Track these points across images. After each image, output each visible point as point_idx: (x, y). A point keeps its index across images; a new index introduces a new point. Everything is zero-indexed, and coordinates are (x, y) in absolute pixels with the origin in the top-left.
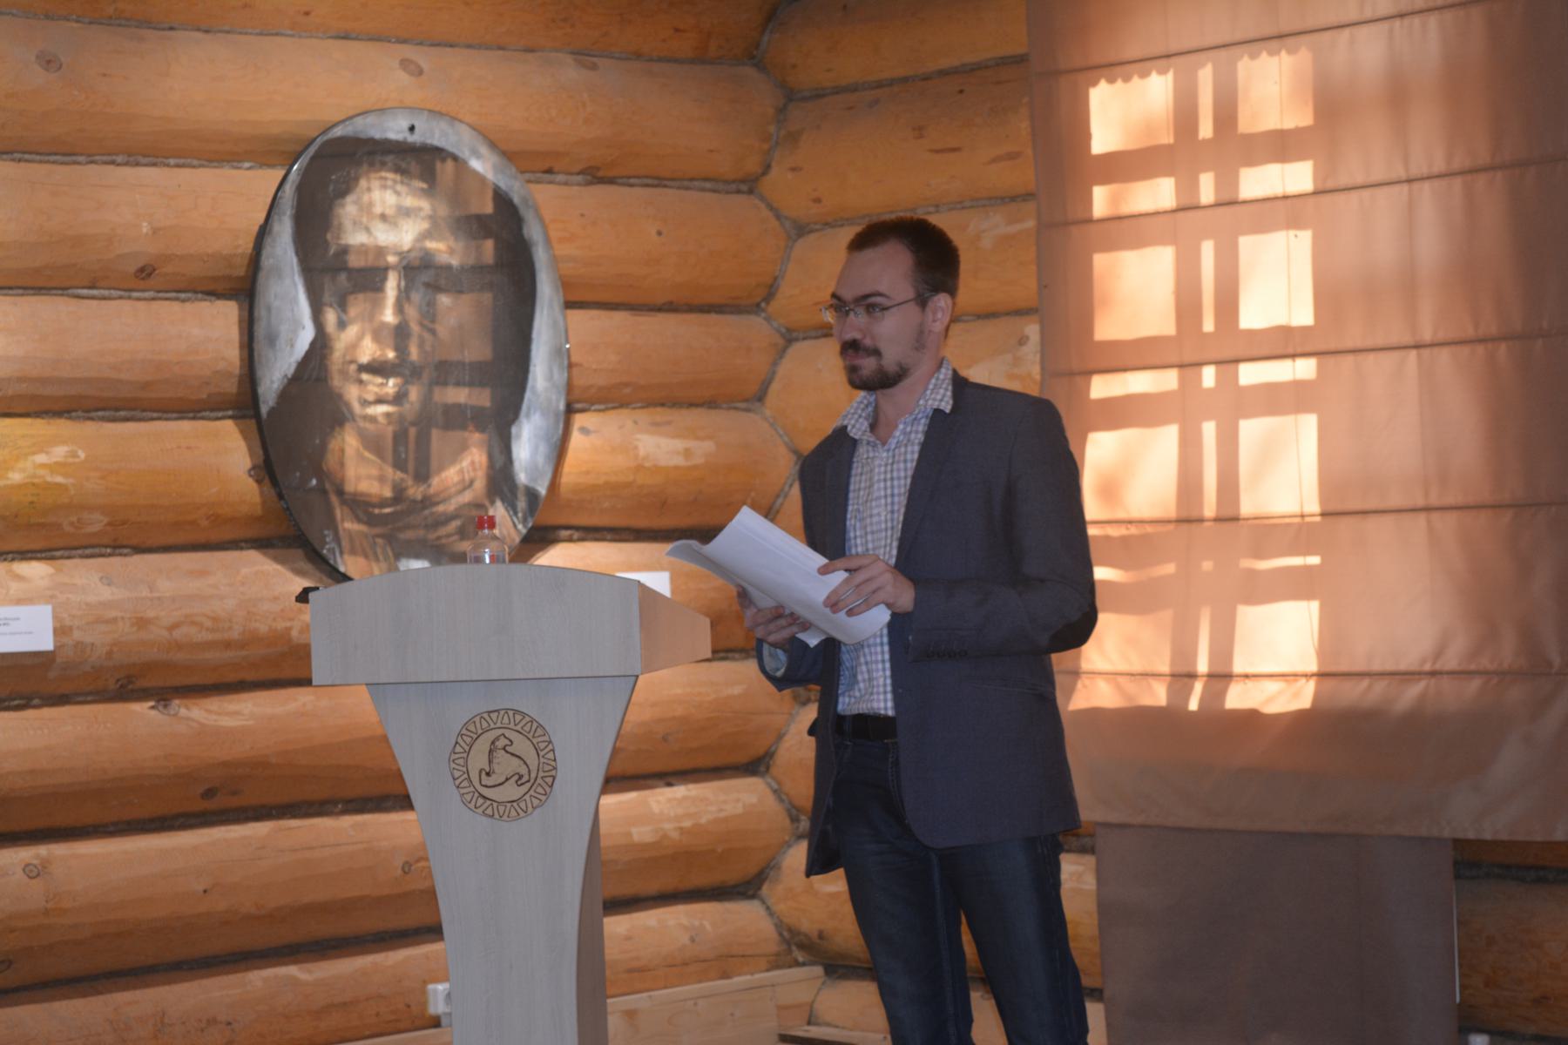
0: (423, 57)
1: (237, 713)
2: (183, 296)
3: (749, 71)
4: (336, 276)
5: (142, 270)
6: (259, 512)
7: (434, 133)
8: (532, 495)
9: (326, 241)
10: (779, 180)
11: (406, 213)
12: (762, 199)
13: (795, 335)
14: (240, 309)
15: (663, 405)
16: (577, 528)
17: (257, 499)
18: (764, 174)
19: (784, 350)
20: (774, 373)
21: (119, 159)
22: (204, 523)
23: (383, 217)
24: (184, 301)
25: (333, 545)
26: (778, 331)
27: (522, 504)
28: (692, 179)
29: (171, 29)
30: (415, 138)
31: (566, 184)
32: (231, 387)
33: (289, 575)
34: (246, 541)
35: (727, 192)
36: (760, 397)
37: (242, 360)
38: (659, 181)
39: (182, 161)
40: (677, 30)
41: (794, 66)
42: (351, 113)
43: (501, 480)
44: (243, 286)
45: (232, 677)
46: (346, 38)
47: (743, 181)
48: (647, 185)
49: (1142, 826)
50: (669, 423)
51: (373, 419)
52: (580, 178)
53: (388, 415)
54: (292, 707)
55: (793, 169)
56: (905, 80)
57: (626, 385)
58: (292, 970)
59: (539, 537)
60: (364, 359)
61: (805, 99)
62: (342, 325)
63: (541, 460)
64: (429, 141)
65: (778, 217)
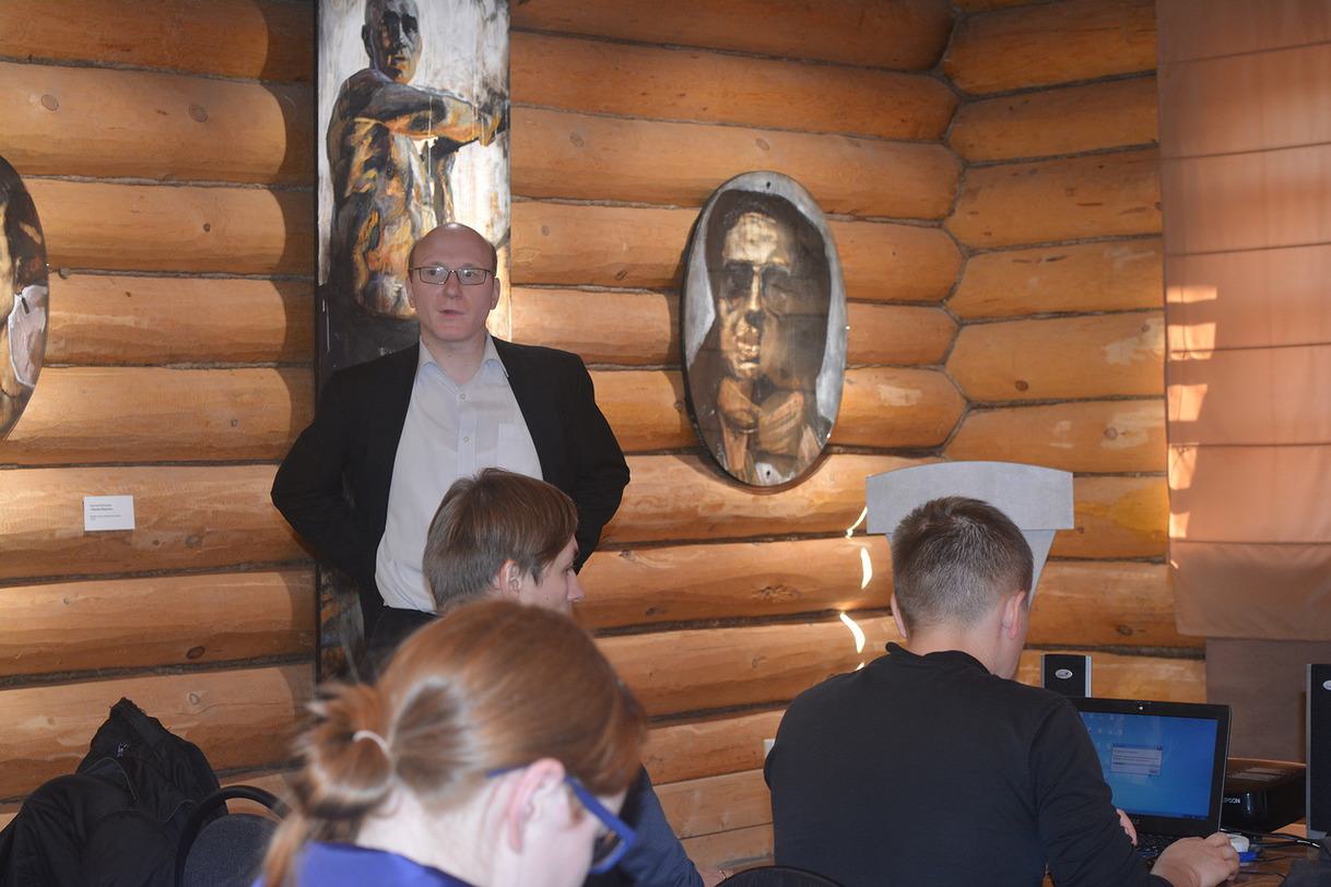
0: (768, 137)
1: (666, 560)
2: (637, 290)
3: (941, 148)
4: (732, 279)
5: (619, 274)
6: (679, 431)
7: (782, 189)
8: (828, 425)
9: (721, 256)
10: (961, 222)
11: (766, 239)
12: (947, 232)
13: (965, 321)
14: (668, 299)
15: (889, 366)
16: (842, 445)
17: (679, 423)
18: (950, 215)
19: (958, 331)
20: (952, 347)
21: (607, 203)
22: (649, 437)
23: (752, 241)
24: (637, 294)
25: (722, 453)
26: (954, 318)
27: (821, 429)
28: (907, 218)
29: (633, 119)
30: (768, 191)
31: (840, 220)
32: (664, 350)
33: (694, 472)
34: (668, 449)
35: (928, 227)
36: (943, 362)
37: (672, 332)
38: (888, 219)
39: (638, 204)
40: (903, 121)
41: (971, 146)
42: (735, 174)
43: (810, 411)
44: (675, 286)
45: (662, 537)
46: (723, 124)
47: (936, 220)
48: (883, 222)
49: (1242, 639)
50: (894, 378)
51: (743, 372)
52: (847, 217)
53: (752, 369)
54: (694, 557)
55: (972, 213)
56: (1055, 157)
57: (872, 352)
58: (688, 728)
59: (826, 453)
60: (740, 334)
61: (978, 167)
62: (729, 311)
63: (832, 400)
64: (777, 193)
65: (958, 244)
